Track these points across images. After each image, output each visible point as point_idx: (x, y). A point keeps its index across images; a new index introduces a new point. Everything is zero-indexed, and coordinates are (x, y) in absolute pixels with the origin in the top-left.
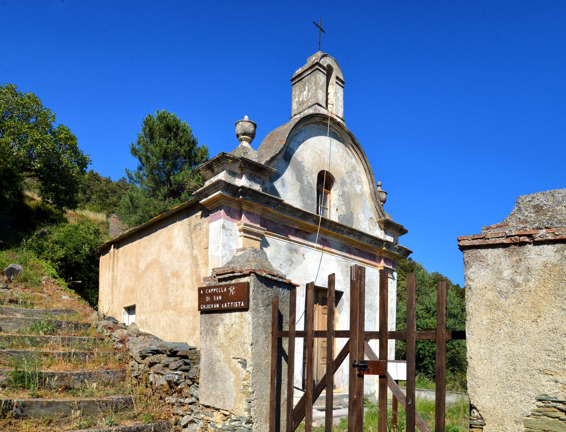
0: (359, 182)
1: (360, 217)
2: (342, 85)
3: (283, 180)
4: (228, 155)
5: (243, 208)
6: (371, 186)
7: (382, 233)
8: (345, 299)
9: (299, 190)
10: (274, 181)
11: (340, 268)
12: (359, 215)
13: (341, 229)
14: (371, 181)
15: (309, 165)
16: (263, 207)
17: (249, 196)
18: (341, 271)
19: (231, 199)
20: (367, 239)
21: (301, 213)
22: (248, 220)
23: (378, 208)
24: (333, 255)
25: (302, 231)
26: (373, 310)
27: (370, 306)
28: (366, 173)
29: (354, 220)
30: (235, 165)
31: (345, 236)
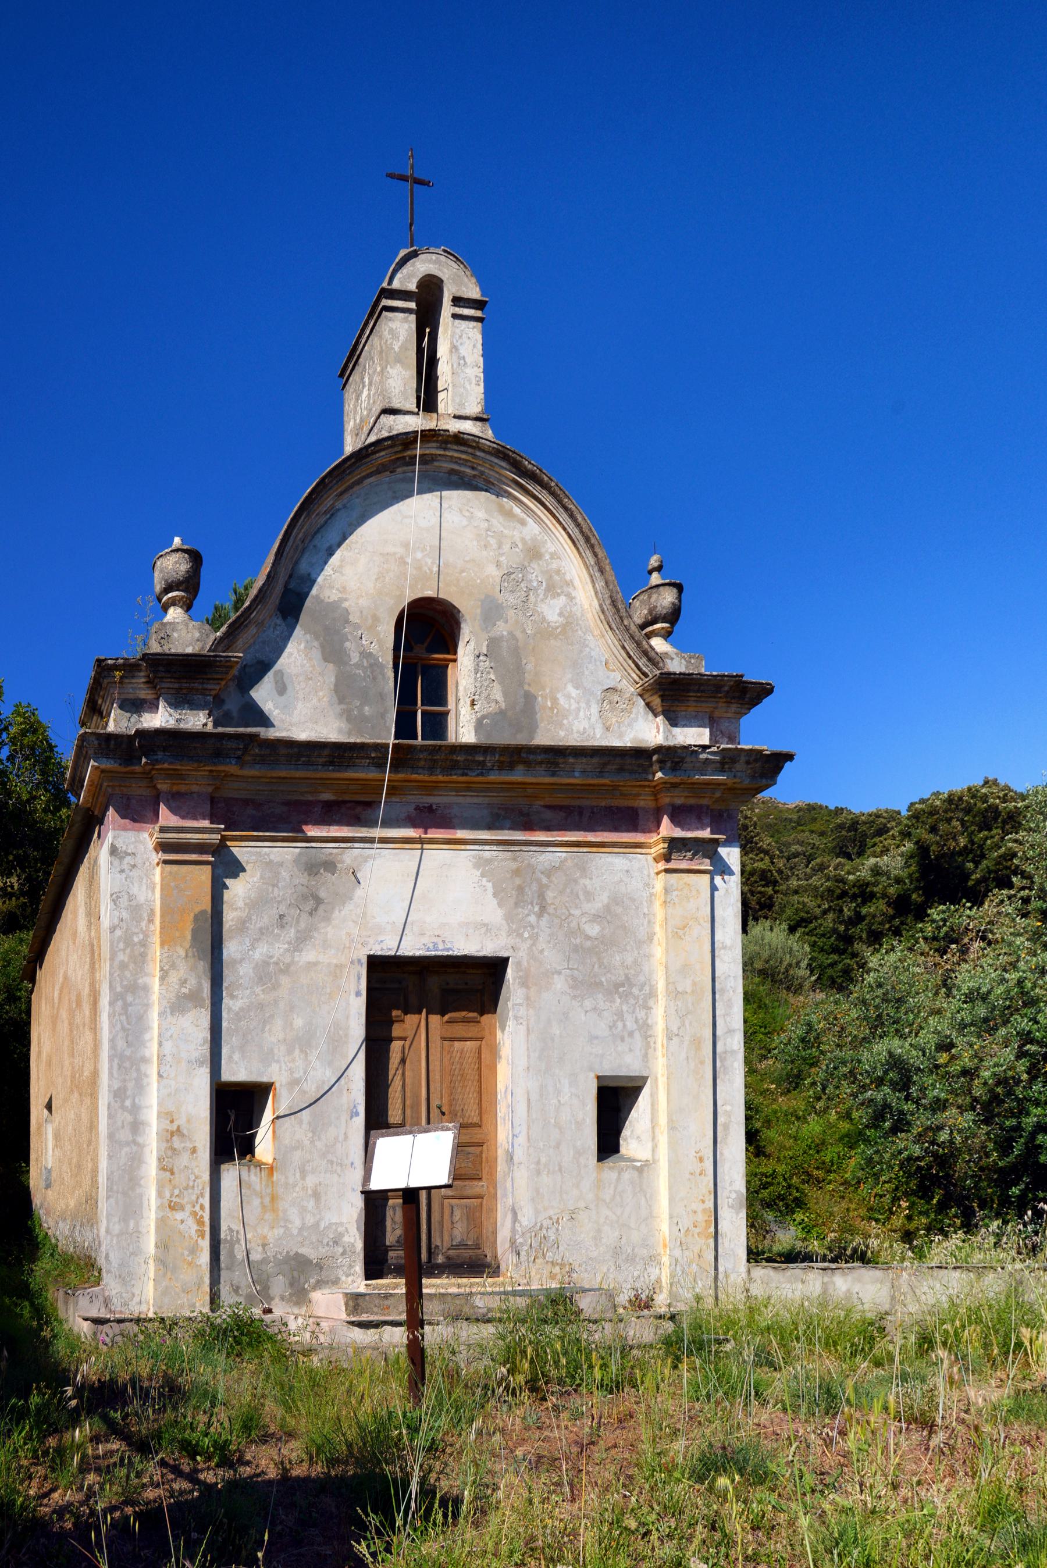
0: (555, 586)
1: (562, 701)
2: (478, 314)
3: (280, 673)
4: (110, 662)
5: (159, 786)
6: (600, 584)
7: (658, 727)
8: (514, 979)
9: (332, 687)
10: (251, 687)
11: (489, 885)
12: (559, 696)
13: (474, 761)
14: (596, 568)
15: (363, 602)
16: (206, 768)
17: (164, 751)
18: (495, 895)
19: (126, 773)
20: (581, 763)
21: (326, 752)
22: (175, 814)
23: (630, 646)
24: (463, 847)
25: (344, 802)
26: (636, 998)
27: (623, 985)
28: (578, 549)
29: (538, 716)
30: (134, 681)
31: (493, 777)
